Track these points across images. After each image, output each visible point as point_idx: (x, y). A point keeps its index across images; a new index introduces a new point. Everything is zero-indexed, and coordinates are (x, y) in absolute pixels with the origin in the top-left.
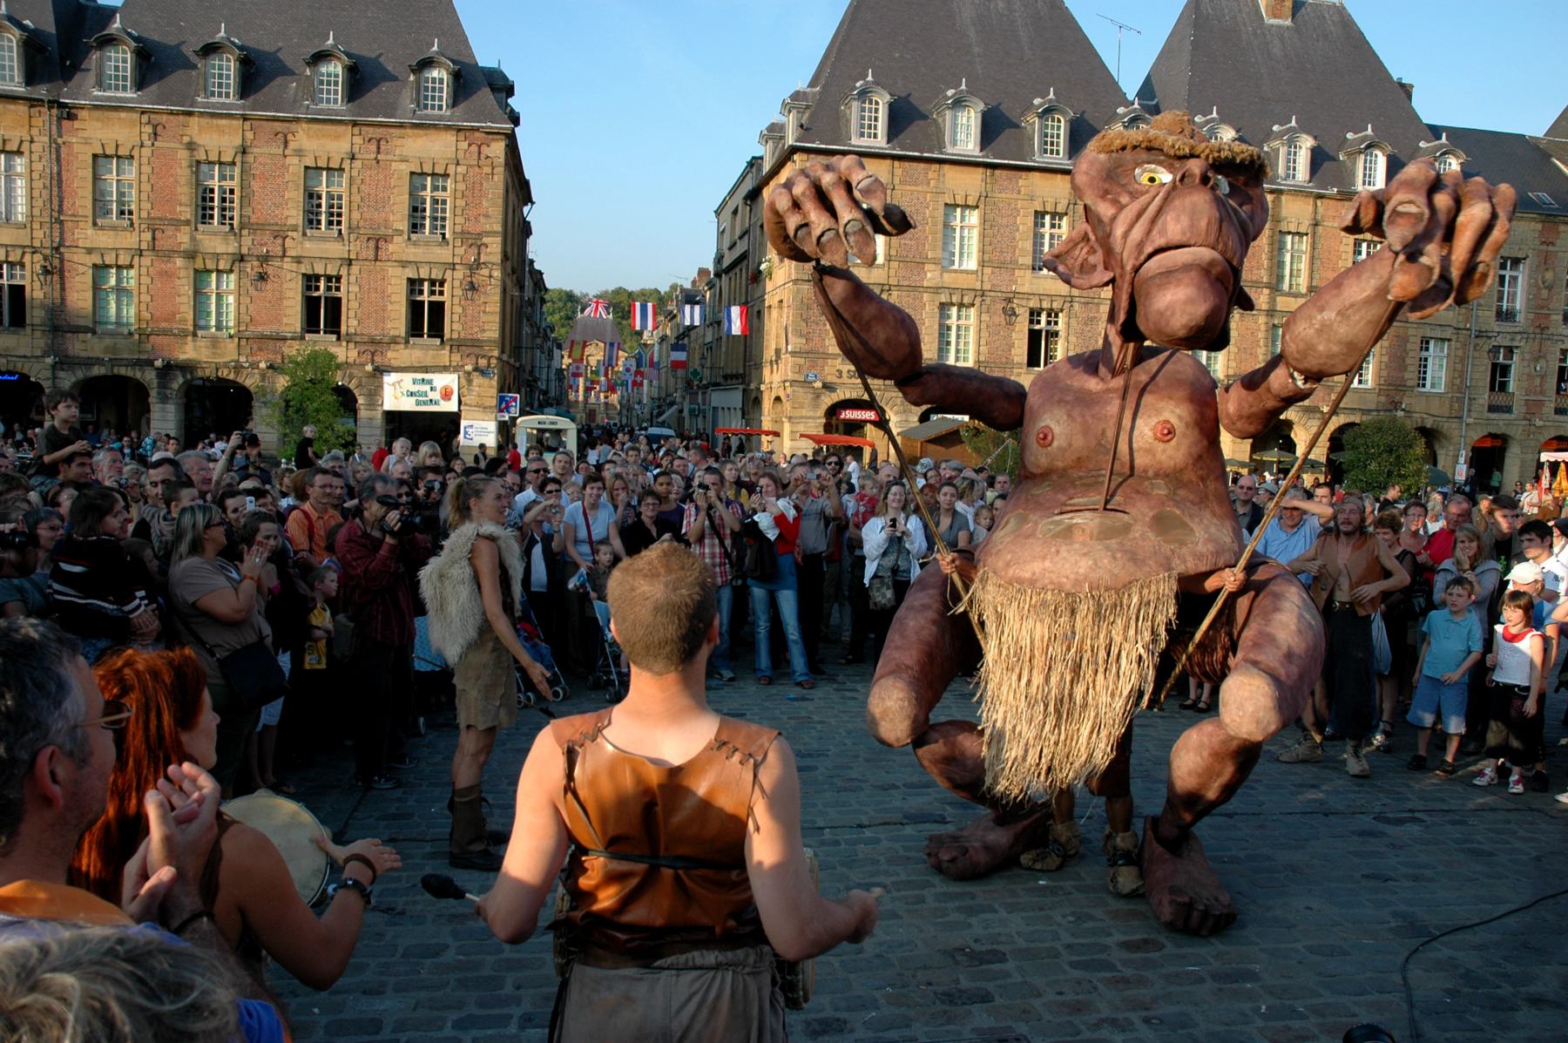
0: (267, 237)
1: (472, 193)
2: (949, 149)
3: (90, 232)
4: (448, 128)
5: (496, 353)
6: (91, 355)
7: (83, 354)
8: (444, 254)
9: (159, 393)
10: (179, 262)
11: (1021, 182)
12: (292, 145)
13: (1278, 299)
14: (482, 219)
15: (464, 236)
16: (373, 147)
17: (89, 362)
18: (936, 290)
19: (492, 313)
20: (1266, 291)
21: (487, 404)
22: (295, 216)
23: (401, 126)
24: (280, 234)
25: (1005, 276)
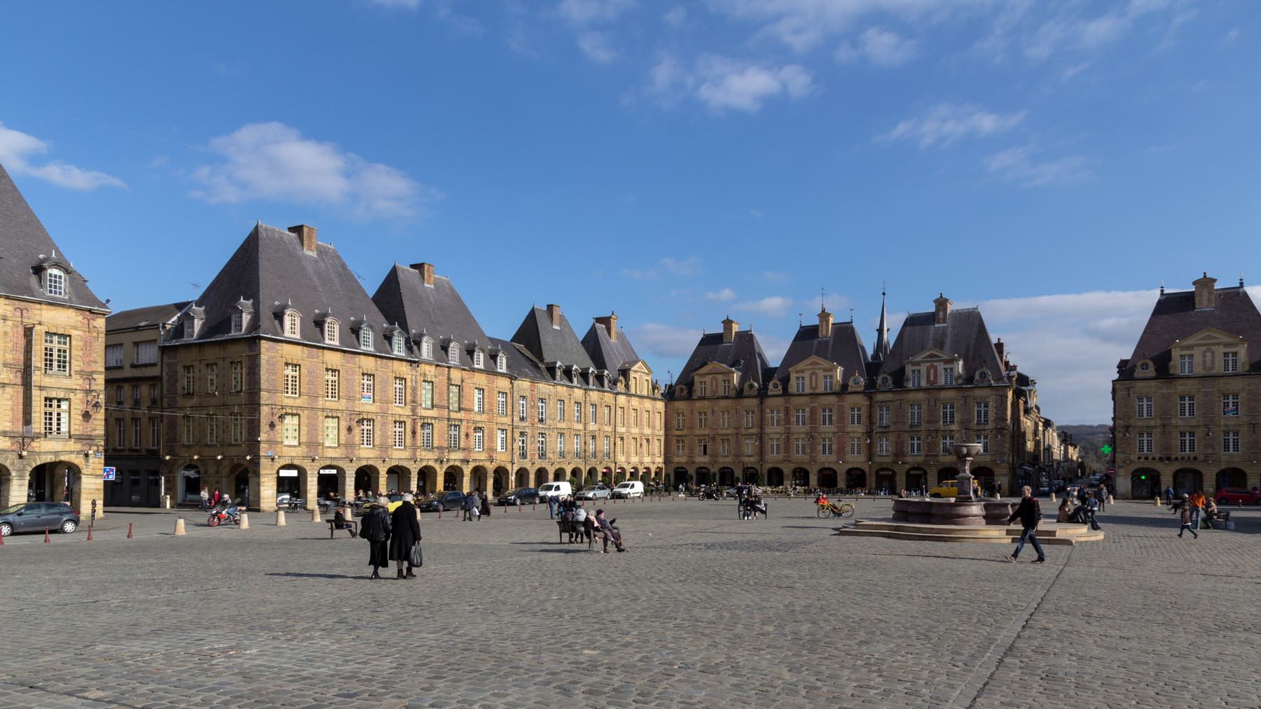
2: (327, 341)
5: (103, 443)
11: (357, 359)
13: (451, 413)
18: (323, 410)
19: (100, 420)
20: (447, 410)
21: (98, 473)
25: (351, 403)
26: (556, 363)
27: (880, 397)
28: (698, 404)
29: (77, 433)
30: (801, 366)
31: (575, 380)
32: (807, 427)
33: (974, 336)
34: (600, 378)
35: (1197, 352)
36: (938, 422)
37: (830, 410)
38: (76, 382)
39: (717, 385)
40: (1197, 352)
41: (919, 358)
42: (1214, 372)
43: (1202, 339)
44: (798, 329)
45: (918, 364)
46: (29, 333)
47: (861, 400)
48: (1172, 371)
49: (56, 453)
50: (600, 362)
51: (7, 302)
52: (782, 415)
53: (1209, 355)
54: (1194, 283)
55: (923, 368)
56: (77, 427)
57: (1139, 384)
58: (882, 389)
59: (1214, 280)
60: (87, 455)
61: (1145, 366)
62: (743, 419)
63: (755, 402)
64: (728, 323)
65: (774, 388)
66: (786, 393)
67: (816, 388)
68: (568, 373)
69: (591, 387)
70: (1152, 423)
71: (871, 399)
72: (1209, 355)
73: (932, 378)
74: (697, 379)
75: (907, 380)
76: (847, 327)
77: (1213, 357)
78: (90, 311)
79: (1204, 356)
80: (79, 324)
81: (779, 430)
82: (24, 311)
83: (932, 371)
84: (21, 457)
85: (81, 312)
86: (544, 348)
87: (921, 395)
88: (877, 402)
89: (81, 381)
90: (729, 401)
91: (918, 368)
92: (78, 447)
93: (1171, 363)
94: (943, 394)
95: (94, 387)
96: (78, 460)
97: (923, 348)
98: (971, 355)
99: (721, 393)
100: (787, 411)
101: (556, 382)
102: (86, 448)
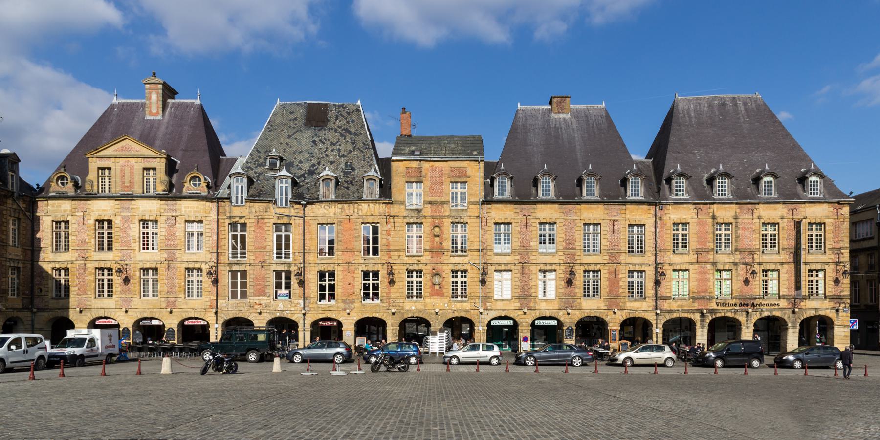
0: (746, 254)
1: (837, 228)
3: (671, 256)
4: (825, 202)
5: (849, 301)
6: (672, 309)
7: (669, 309)
8: (824, 258)
9: (701, 324)
10: (709, 267)
12: (756, 214)
14: (841, 242)
15: (832, 250)
16: (791, 213)
17: (671, 312)
19: (847, 284)
21: (846, 324)
22: (758, 244)
23: (804, 203)
24: (752, 252)
29: (831, 294)
38: (829, 257)
46: (798, 225)
49: (816, 310)
51: (784, 206)
56: (830, 290)
60: (838, 311)
78: (839, 203)
80: (831, 214)
82: (795, 211)
84: (794, 312)
85: (832, 205)
89: (832, 256)
92: (832, 304)
95: (842, 260)
96: (831, 314)
102: (837, 305)
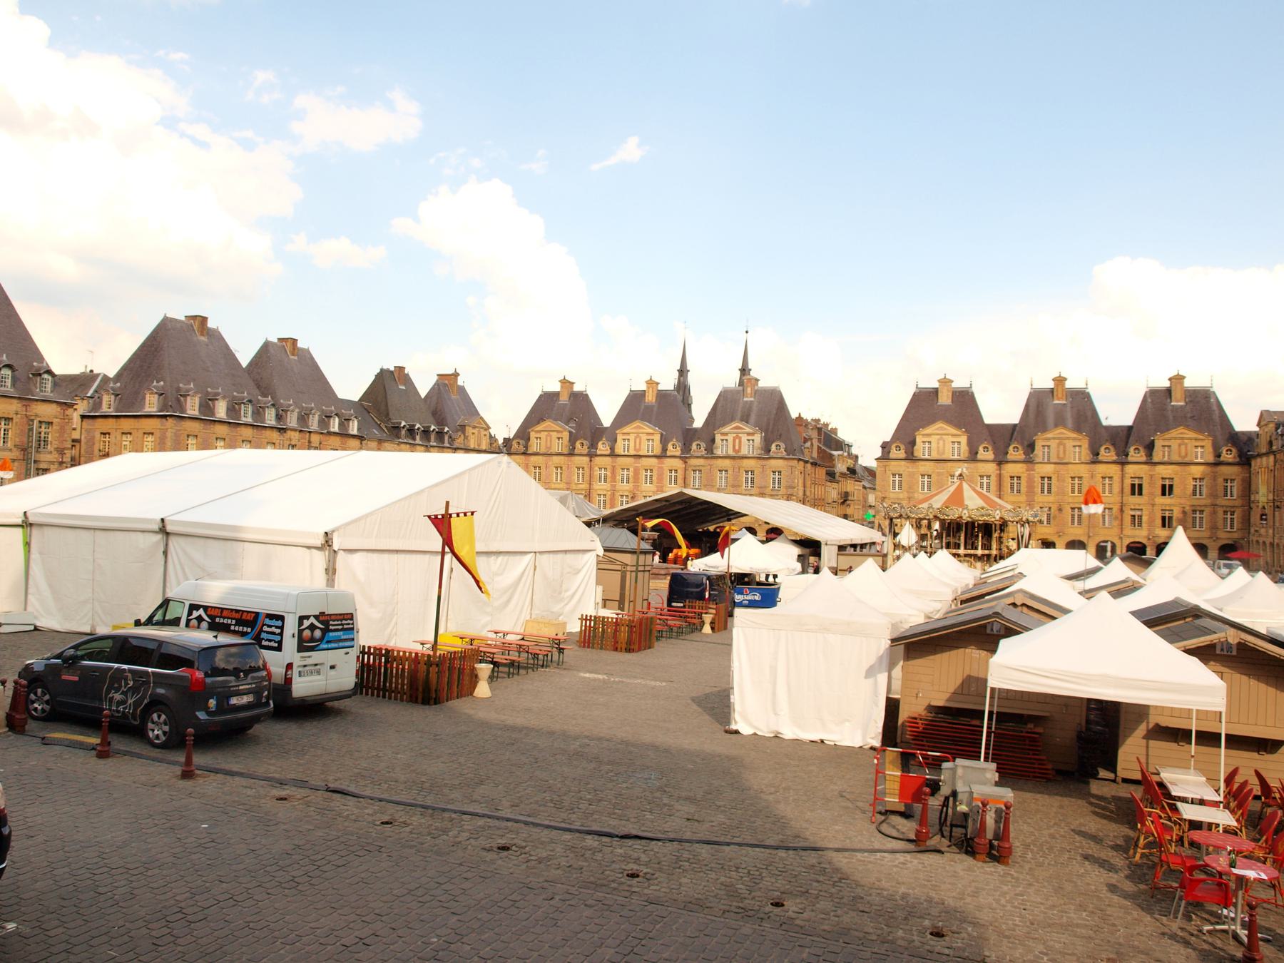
26: (400, 423)
27: (693, 462)
28: (533, 458)
30: (626, 429)
31: (418, 437)
32: (631, 485)
33: (775, 412)
34: (440, 434)
35: (934, 439)
36: (740, 486)
37: (651, 470)
39: (551, 441)
40: (934, 439)
41: (726, 429)
42: (944, 457)
43: (937, 429)
44: (628, 392)
45: (726, 434)
47: (677, 463)
48: (915, 454)
50: (441, 421)
52: (609, 473)
53: (941, 442)
54: (939, 381)
55: (730, 438)
57: (893, 463)
58: (696, 454)
59: (952, 382)
61: (898, 448)
62: (574, 475)
63: (586, 459)
64: (565, 383)
65: (603, 448)
66: (613, 454)
67: (639, 450)
68: (411, 431)
69: (433, 443)
70: (901, 496)
71: (686, 462)
72: (941, 442)
73: (737, 447)
74: (533, 435)
75: (717, 448)
76: (670, 395)
77: (944, 444)
79: (938, 443)
81: (605, 487)
83: (737, 441)
86: (390, 408)
87: (727, 463)
88: (691, 466)
90: (562, 457)
91: (725, 438)
93: (915, 448)
94: (746, 463)
97: (732, 420)
98: (771, 428)
99: (555, 449)
100: (614, 468)
101: (400, 440)
